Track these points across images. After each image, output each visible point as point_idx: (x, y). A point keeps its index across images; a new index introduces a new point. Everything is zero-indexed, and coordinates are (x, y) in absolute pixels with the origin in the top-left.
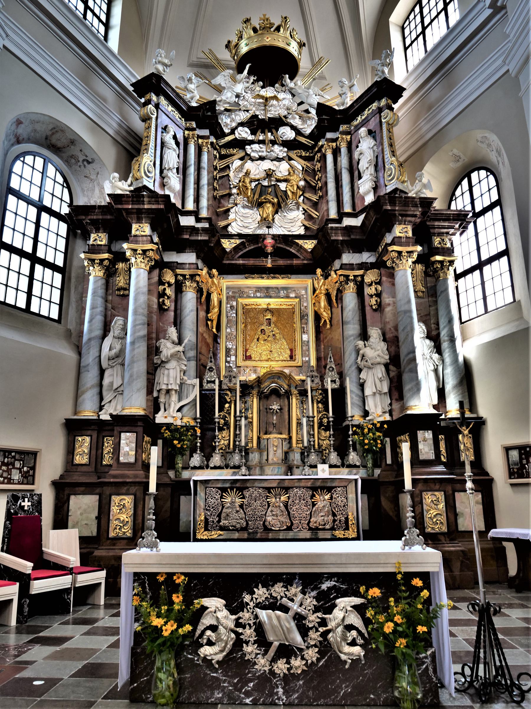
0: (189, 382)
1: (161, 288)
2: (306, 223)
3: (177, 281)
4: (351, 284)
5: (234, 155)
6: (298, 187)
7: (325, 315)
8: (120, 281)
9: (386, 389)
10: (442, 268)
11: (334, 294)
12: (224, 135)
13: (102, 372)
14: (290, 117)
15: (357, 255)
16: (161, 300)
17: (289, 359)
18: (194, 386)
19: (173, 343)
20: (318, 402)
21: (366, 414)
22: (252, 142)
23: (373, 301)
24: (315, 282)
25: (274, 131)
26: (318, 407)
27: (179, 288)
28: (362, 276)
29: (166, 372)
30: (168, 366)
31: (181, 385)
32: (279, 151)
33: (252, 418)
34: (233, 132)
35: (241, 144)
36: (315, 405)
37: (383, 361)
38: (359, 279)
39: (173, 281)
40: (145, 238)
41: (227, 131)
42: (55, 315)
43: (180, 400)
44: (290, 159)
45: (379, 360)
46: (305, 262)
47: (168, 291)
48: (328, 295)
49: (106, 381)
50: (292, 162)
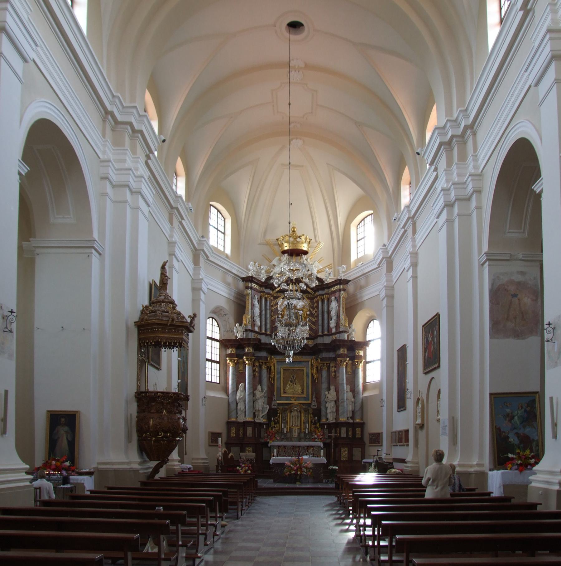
0: (265, 406)
1: (254, 368)
2: (310, 332)
3: (259, 365)
4: (325, 367)
5: (279, 297)
6: (307, 314)
7: (315, 376)
8: (241, 368)
9: (334, 411)
10: (357, 364)
11: (319, 368)
12: (276, 288)
13: (237, 404)
14: (304, 278)
15: (328, 353)
16: (254, 373)
17: (301, 393)
18: (267, 408)
19: (260, 392)
20: (311, 414)
21: (327, 419)
22: (287, 291)
23: (333, 374)
24: (312, 361)
25: (297, 284)
26: (311, 416)
27: (260, 367)
28: (330, 364)
29: (258, 403)
30: (258, 401)
31: (263, 407)
32: (299, 295)
33: (288, 420)
34: (279, 286)
35: (283, 291)
36: (310, 415)
37: (334, 400)
38: (328, 364)
39: (258, 365)
40: (251, 354)
41: (276, 286)
42: (218, 382)
43: (262, 413)
44: (304, 299)
45: (332, 399)
46: (309, 351)
47: (257, 370)
48: (317, 368)
49: (239, 407)
50: (304, 301)
